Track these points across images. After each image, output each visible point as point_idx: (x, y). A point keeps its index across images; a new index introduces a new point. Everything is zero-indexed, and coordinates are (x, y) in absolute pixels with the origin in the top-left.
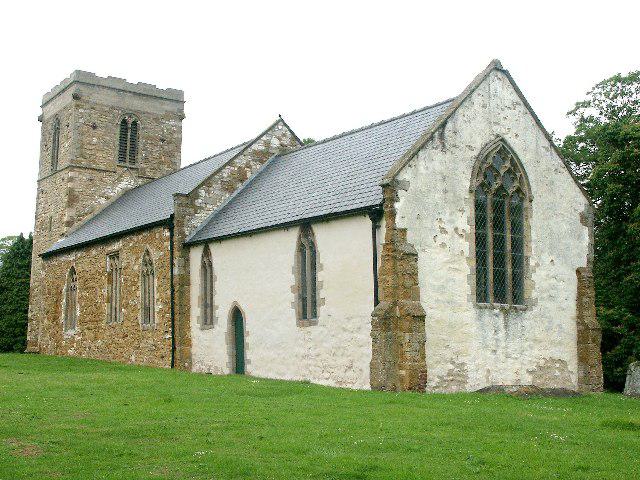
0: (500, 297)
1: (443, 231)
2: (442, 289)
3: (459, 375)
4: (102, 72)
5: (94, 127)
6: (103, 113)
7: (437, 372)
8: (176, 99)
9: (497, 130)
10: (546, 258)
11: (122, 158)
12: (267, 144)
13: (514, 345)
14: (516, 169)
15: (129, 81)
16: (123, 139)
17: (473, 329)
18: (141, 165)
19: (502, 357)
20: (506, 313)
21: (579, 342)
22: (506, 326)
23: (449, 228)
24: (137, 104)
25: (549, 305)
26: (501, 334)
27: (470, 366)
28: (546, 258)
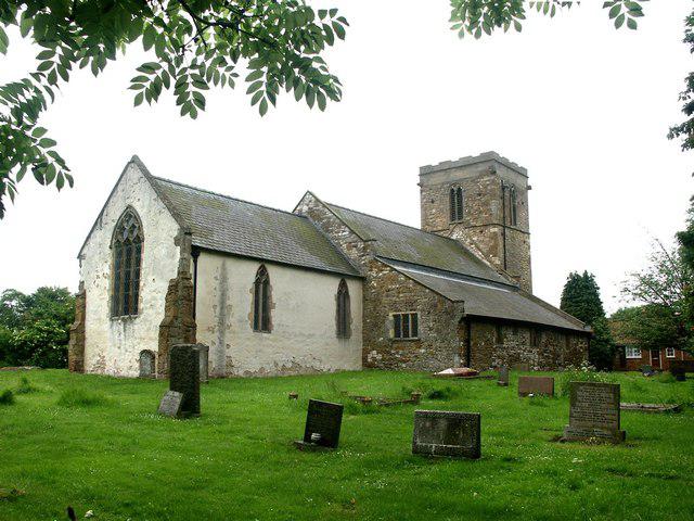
0: (126, 312)
1: (98, 277)
2: (96, 312)
3: (101, 364)
4: (435, 163)
5: (433, 202)
6: (437, 190)
7: (90, 363)
8: (426, 172)
9: (128, 202)
10: (150, 278)
11: (453, 218)
12: (300, 211)
13: (129, 343)
14: (137, 218)
15: (474, 156)
16: (460, 202)
17: (108, 335)
18: (466, 218)
19: (123, 351)
20: (124, 321)
21: (84, 339)
22: (125, 330)
23: (100, 274)
24: (459, 175)
25: (151, 311)
26: (122, 336)
27: (107, 358)
28: (150, 278)
